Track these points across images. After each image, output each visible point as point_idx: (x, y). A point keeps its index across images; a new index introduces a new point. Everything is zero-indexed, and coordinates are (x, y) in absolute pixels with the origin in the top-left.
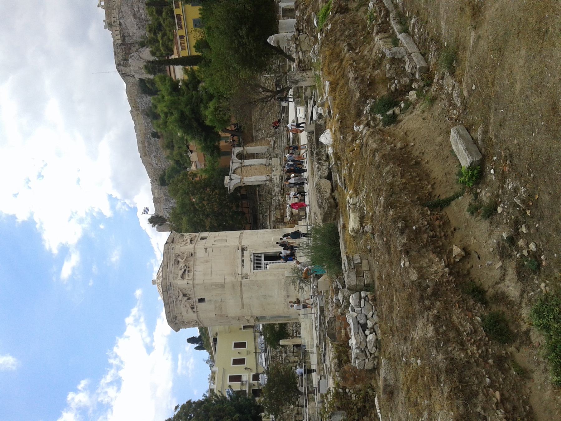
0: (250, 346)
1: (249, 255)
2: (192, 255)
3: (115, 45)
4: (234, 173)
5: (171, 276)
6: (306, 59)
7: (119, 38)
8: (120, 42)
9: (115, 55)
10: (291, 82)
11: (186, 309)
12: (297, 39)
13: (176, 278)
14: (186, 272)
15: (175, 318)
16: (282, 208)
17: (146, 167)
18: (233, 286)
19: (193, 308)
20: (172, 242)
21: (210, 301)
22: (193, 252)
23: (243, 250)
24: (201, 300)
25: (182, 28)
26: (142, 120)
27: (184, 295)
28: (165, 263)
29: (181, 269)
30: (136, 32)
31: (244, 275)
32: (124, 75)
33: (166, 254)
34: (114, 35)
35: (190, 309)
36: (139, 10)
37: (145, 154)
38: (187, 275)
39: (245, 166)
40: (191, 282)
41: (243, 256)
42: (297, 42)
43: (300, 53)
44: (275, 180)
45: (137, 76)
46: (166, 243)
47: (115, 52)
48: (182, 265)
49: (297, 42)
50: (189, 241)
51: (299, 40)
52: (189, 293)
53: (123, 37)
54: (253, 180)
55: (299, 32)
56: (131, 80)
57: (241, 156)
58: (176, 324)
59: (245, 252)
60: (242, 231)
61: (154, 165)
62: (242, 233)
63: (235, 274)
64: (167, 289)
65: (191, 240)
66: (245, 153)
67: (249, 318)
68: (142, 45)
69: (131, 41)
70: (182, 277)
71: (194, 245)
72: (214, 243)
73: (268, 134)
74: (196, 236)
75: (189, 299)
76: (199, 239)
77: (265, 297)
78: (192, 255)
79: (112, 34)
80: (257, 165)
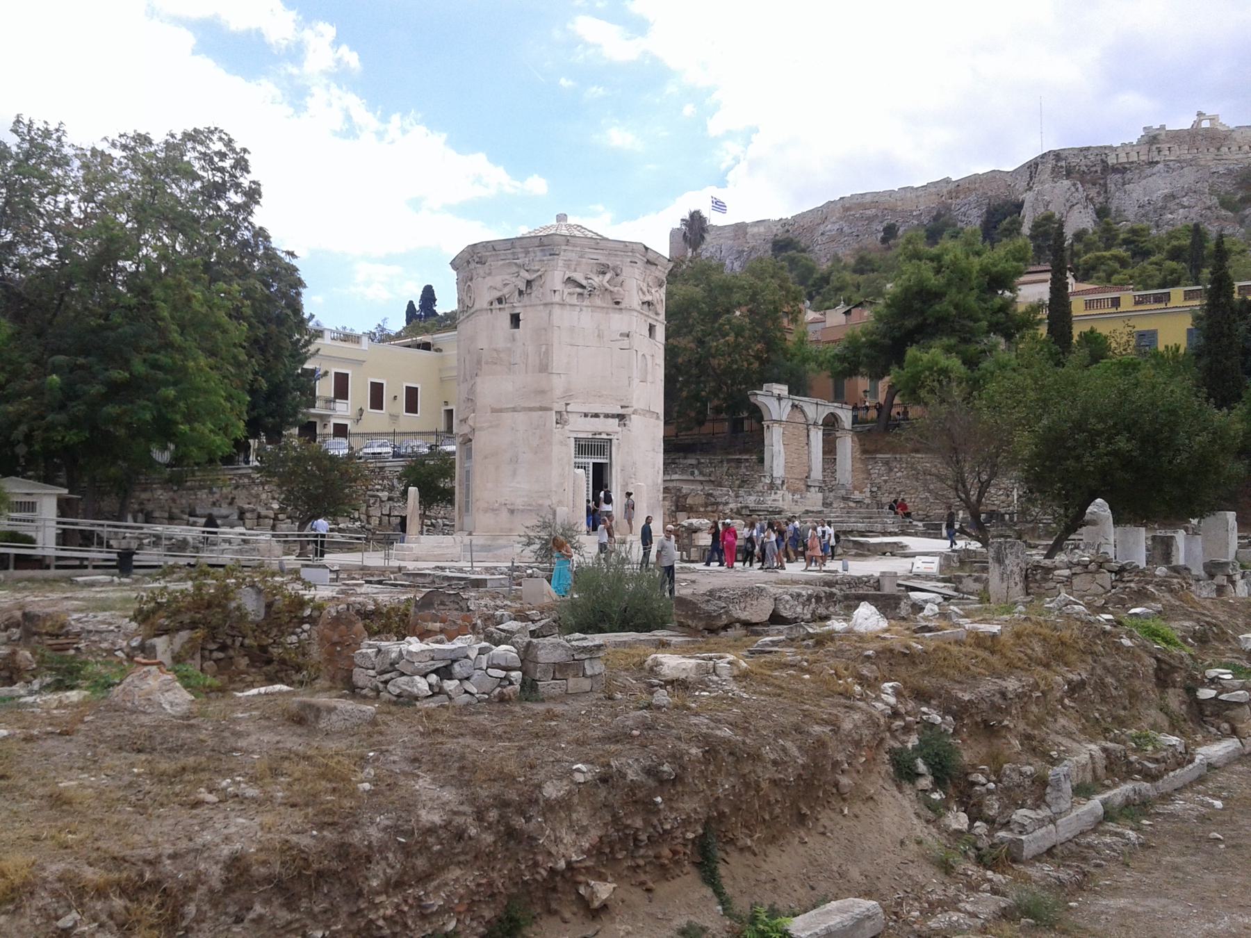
0: (409, 422)
1: (609, 430)
2: (617, 303)
3: (1104, 151)
4: (794, 406)
5: (573, 256)
6: (1052, 584)
8: (1111, 160)
9: (1081, 150)
10: (999, 547)
11: (499, 285)
12: (1100, 567)
13: (569, 267)
14: (579, 290)
15: (481, 262)
16: (709, 509)
17: (817, 209)
18: (543, 392)
19: (500, 300)
20: (648, 262)
22: (622, 306)
23: (621, 417)
24: (515, 320)
25: (1137, 303)
26: (927, 204)
27: (529, 283)
28: (602, 243)
29: (587, 278)
30: (1131, 201)
31: (565, 416)
32: (1033, 167)
33: (621, 246)
35: (498, 294)
36: (1184, 207)
37: (847, 209)
38: (571, 290)
40: (557, 298)
41: (607, 416)
42: (1092, 567)
43: (1067, 572)
44: (773, 497)
45: (1028, 197)
46: (646, 249)
47: (1088, 149)
48: (597, 280)
49: (1092, 567)
50: (648, 298)
51: (1097, 572)
53: (1121, 169)
54: (776, 448)
55: (1116, 573)
56: (1022, 184)
57: (831, 424)
58: (468, 262)
60: (662, 417)
61: (822, 228)
62: (658, 418)
63: (568, 397)
64: (544, 245)
65: (649, 303)
66: (838, 434)
67: (470, 422)
68: (1102, 213)
69: (1111, 187)
70: (570, 281)
71: (639, 308)
72: (640, 354)
73: (879, 488)
74: (657, 314)
75: (521, 293)
76: (650, 321)
77: (514, 460)
78: (617, 303)
80: (809, 459)
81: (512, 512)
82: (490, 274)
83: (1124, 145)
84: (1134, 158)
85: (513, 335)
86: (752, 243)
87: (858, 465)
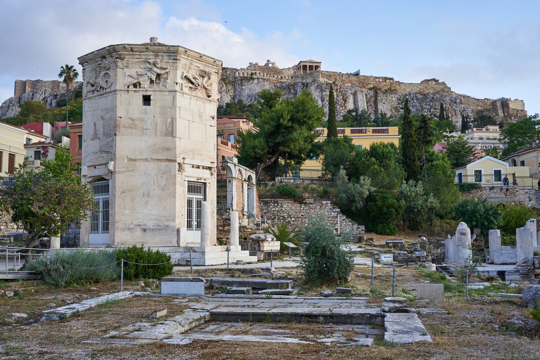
5: (188, 63)
14: (191, 85)
18: (168, 149)
19: (135, 86)
21: (146, 113)
22: (211, 98)
24: (147, 100)
27: (158, 76)
29: (194, 78)
34: (243, 71)
41: (203, 168)
48: (200, 81)
52: (161, 84)
58: (104, 57)
59: (208, 171)
75: (152, 82)
79: (244, 69)
81: (145, 230)
82: (127, 67)
83: (242, 69)
85: (145, 110)
86: (62, 92)
87: (258, 204)
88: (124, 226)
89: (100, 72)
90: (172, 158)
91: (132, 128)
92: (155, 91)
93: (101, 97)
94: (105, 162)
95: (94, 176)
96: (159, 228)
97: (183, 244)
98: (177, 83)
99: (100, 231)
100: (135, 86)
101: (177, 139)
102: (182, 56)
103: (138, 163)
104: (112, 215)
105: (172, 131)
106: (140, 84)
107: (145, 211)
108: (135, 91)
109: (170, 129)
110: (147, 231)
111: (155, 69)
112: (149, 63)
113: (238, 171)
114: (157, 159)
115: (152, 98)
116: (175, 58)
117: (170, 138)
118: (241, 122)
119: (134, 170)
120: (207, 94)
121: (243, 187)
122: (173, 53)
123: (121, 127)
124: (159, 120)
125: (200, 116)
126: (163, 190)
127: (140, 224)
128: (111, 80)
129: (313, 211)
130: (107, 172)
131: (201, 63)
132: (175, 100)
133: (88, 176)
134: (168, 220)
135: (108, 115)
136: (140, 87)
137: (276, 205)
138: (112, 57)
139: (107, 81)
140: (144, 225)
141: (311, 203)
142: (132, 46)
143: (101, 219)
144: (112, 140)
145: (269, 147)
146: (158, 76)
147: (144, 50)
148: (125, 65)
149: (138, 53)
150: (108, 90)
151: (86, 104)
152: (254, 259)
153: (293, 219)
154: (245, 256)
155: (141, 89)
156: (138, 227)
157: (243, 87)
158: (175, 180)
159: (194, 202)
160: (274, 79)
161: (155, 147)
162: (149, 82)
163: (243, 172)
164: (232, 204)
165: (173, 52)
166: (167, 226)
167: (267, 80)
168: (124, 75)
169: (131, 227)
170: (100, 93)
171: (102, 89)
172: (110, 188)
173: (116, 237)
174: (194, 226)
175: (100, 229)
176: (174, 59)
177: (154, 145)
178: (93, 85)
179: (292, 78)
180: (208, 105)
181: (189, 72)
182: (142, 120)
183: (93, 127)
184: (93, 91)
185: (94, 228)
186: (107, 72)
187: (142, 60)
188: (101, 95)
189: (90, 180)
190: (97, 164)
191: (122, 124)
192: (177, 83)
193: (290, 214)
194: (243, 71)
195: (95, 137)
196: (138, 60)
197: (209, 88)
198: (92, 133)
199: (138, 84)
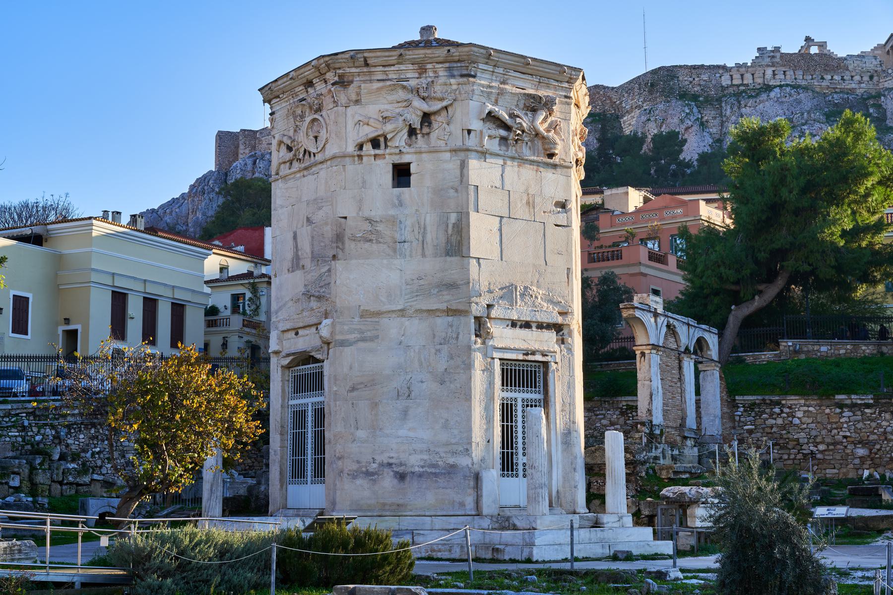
4: (668, 326)
7: (735, 82)
8: (725, 81)
9: (694, 67)
14: (503, 133)
15: (343, 82)
18: (452, 286)
19: (375, 143)
21: (401, 204)
22: (556, 160)
24: (402, 174)
34: (743, 70)
39: (680, 361)
40: (472, 142)
41: (540, 326)
52: (434, 135)
58: (309, 84)
75: (412, 132)
79: (745, 64)
80: (683, 401)
81: (402, 477)
82: (357, 102)
83: (738, 66)
84: (748, 79)
85: (399, 197)
87: (725, 410)
88: (355, 467)
89: (302, 117)
90: (461, 307)
91: (371, 240)
92: (421, 153)
93: (305, 173)
94: (314, 320)
95: (293, 354)
96: (433, 470)
97: (488, 507)
98: (469, 132)
99: (309, 479)
100: (375, 143)
101: (473, 262)
102: (481, 66)
103: (384, 321)
104: (330, 442)
105: (460, 243)
106: (386, 139)
107: (402, 432)
108: (375, 156)
109: (454, 239)
110: (408, 479)
111: (417, 103)
112: (404, 87)
113: (664, 329)
114: (429, 311)
115: (413, 168)
116: (465, 72)
117: (455, 259)
118: (702, 204)
119: (377, 337)
120: (545, 150)
121: (680, 368)
122: (459, 61)
123: (346, 239)
124: (430, 219)
125: (528, 203)
126: (442, 383)
127: (391, 461)
128: (323, 135)
129: (874, 425)
130: (318, 342)
131: (529, 77)
132: (465, 171)
133: (283, 354)
134: (454, 453)
135: (321, 214)
136: (386, 146)
137: (777, 410)
138: (326, 82)
139: (316, 138)
140: (401, 464)
141: (868, 406)
142: (366, 55)
143: (309, 451)
144: (329, 270)
145: (757, 262)
146: (426, 118)
147: (393, 59)
148: (354, 97)
149: (381, 68)
150: (319, 157)
151: (278, 191)
152: (667, 547)
153: (822, 447)
154: (641, 538)
155: (388, 151)
156: (385, 470)
157: (743, 110)
158: (469, 356)
159: (520, 408)
160: (824, 84)
161: (422, 282)
162: (405, 131)
163: (682, 330)
164: (649, 411)
165: (463, 60)
166: (453, 466)
167: (806, 89)
168: (349, 122)
169: (371, 470)
170: (303, 166)
171: (307, 156)
172: (326, 379)
173: (338, 493)
174: (521, 467)
175: (309, 473)
176: (462, 76)
177: (420, 279)
178: (290, 149)
179: (871, 77)
180: (549, 175)
181: (500, 103)
182: (393, 221)
183: (291, 242)
184: (291, 162)
185: (298, 473)
186: (316, 116)
187: (388, 83)
188: (306, 169)
189: (286, 361)
190: (301, 325)
191: (348, 233)
192: (469, 132)
193: (814, 433)
194: (743, 70)
195: (296, 264)
196: (381, 84)
197: (551, 134)
198: (289, 255)
199: (382, 139)
